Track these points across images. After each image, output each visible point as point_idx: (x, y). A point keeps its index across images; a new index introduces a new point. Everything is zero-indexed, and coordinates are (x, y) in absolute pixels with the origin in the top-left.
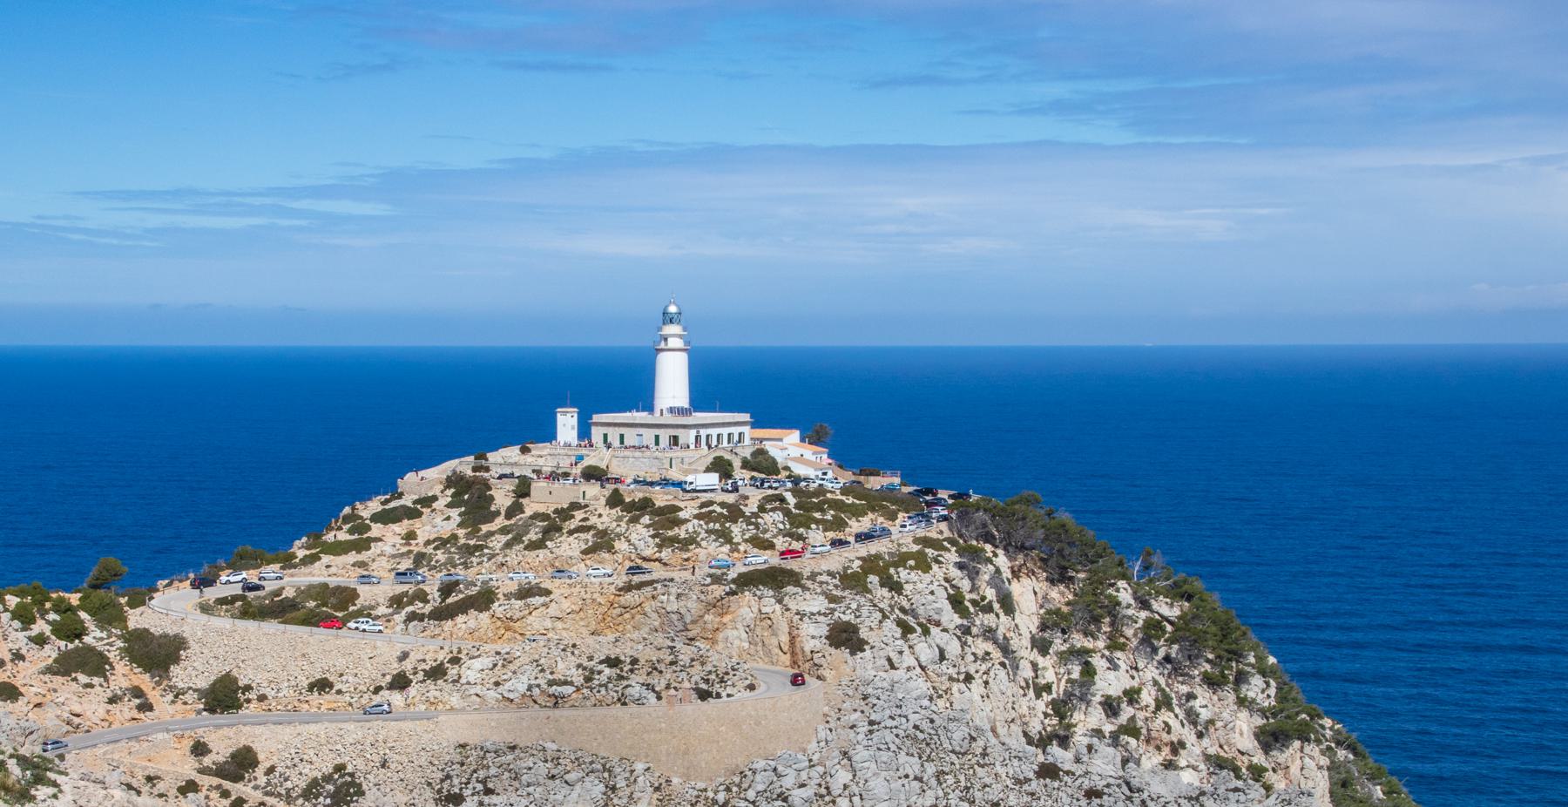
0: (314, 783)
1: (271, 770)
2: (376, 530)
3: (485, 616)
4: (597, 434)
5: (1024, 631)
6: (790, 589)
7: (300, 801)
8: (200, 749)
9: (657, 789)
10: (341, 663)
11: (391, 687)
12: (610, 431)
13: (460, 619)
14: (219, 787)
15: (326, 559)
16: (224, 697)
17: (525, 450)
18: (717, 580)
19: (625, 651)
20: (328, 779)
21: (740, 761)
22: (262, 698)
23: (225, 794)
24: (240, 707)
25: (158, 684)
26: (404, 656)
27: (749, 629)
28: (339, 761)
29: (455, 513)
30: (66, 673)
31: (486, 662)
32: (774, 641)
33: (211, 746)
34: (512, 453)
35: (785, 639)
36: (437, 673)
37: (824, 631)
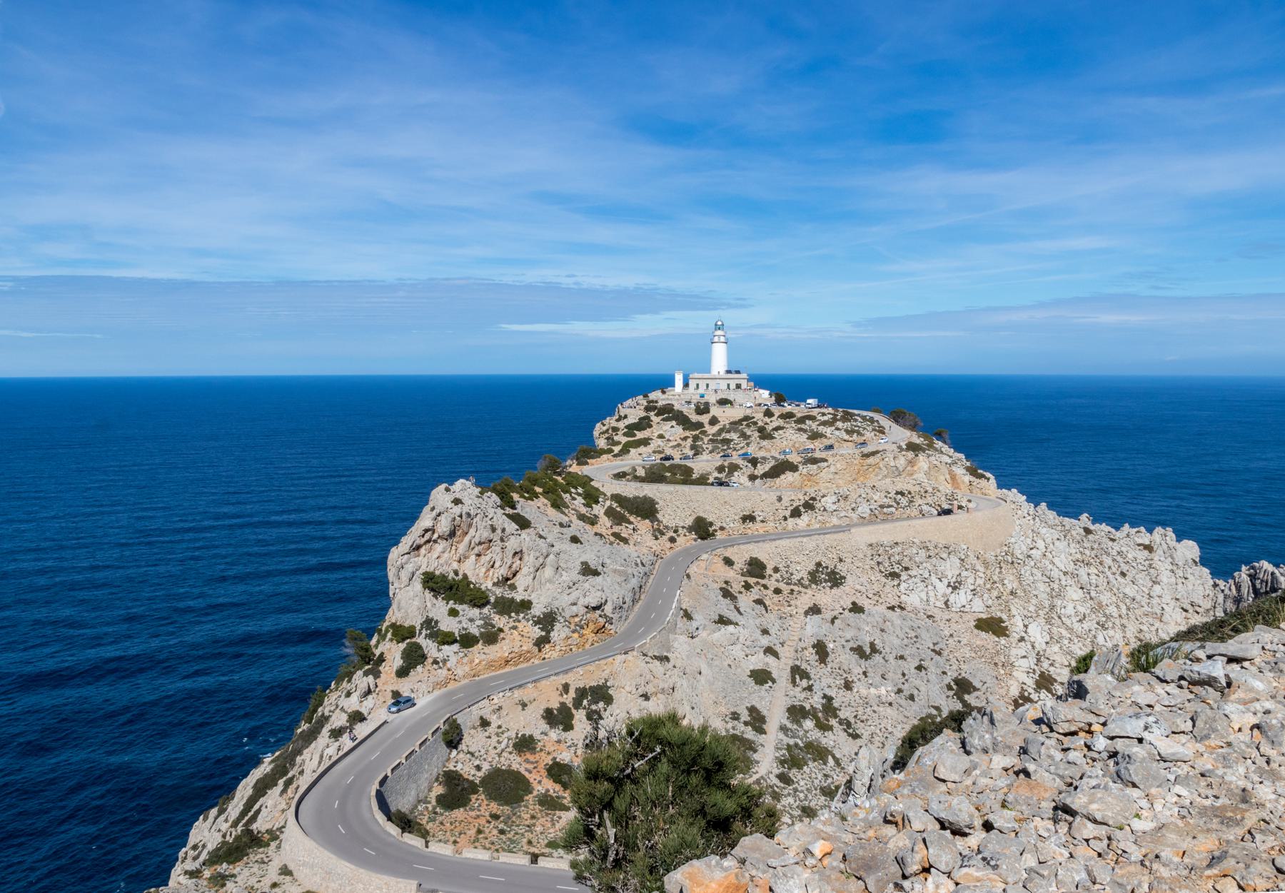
1: (776, 570)
3: (796, 474)
8: (728, 562)
10: (748, 505)
12: (700, 382)
17: (664, 392)
23: (765, 587)
32: (942, 478)
35: (948, 477)
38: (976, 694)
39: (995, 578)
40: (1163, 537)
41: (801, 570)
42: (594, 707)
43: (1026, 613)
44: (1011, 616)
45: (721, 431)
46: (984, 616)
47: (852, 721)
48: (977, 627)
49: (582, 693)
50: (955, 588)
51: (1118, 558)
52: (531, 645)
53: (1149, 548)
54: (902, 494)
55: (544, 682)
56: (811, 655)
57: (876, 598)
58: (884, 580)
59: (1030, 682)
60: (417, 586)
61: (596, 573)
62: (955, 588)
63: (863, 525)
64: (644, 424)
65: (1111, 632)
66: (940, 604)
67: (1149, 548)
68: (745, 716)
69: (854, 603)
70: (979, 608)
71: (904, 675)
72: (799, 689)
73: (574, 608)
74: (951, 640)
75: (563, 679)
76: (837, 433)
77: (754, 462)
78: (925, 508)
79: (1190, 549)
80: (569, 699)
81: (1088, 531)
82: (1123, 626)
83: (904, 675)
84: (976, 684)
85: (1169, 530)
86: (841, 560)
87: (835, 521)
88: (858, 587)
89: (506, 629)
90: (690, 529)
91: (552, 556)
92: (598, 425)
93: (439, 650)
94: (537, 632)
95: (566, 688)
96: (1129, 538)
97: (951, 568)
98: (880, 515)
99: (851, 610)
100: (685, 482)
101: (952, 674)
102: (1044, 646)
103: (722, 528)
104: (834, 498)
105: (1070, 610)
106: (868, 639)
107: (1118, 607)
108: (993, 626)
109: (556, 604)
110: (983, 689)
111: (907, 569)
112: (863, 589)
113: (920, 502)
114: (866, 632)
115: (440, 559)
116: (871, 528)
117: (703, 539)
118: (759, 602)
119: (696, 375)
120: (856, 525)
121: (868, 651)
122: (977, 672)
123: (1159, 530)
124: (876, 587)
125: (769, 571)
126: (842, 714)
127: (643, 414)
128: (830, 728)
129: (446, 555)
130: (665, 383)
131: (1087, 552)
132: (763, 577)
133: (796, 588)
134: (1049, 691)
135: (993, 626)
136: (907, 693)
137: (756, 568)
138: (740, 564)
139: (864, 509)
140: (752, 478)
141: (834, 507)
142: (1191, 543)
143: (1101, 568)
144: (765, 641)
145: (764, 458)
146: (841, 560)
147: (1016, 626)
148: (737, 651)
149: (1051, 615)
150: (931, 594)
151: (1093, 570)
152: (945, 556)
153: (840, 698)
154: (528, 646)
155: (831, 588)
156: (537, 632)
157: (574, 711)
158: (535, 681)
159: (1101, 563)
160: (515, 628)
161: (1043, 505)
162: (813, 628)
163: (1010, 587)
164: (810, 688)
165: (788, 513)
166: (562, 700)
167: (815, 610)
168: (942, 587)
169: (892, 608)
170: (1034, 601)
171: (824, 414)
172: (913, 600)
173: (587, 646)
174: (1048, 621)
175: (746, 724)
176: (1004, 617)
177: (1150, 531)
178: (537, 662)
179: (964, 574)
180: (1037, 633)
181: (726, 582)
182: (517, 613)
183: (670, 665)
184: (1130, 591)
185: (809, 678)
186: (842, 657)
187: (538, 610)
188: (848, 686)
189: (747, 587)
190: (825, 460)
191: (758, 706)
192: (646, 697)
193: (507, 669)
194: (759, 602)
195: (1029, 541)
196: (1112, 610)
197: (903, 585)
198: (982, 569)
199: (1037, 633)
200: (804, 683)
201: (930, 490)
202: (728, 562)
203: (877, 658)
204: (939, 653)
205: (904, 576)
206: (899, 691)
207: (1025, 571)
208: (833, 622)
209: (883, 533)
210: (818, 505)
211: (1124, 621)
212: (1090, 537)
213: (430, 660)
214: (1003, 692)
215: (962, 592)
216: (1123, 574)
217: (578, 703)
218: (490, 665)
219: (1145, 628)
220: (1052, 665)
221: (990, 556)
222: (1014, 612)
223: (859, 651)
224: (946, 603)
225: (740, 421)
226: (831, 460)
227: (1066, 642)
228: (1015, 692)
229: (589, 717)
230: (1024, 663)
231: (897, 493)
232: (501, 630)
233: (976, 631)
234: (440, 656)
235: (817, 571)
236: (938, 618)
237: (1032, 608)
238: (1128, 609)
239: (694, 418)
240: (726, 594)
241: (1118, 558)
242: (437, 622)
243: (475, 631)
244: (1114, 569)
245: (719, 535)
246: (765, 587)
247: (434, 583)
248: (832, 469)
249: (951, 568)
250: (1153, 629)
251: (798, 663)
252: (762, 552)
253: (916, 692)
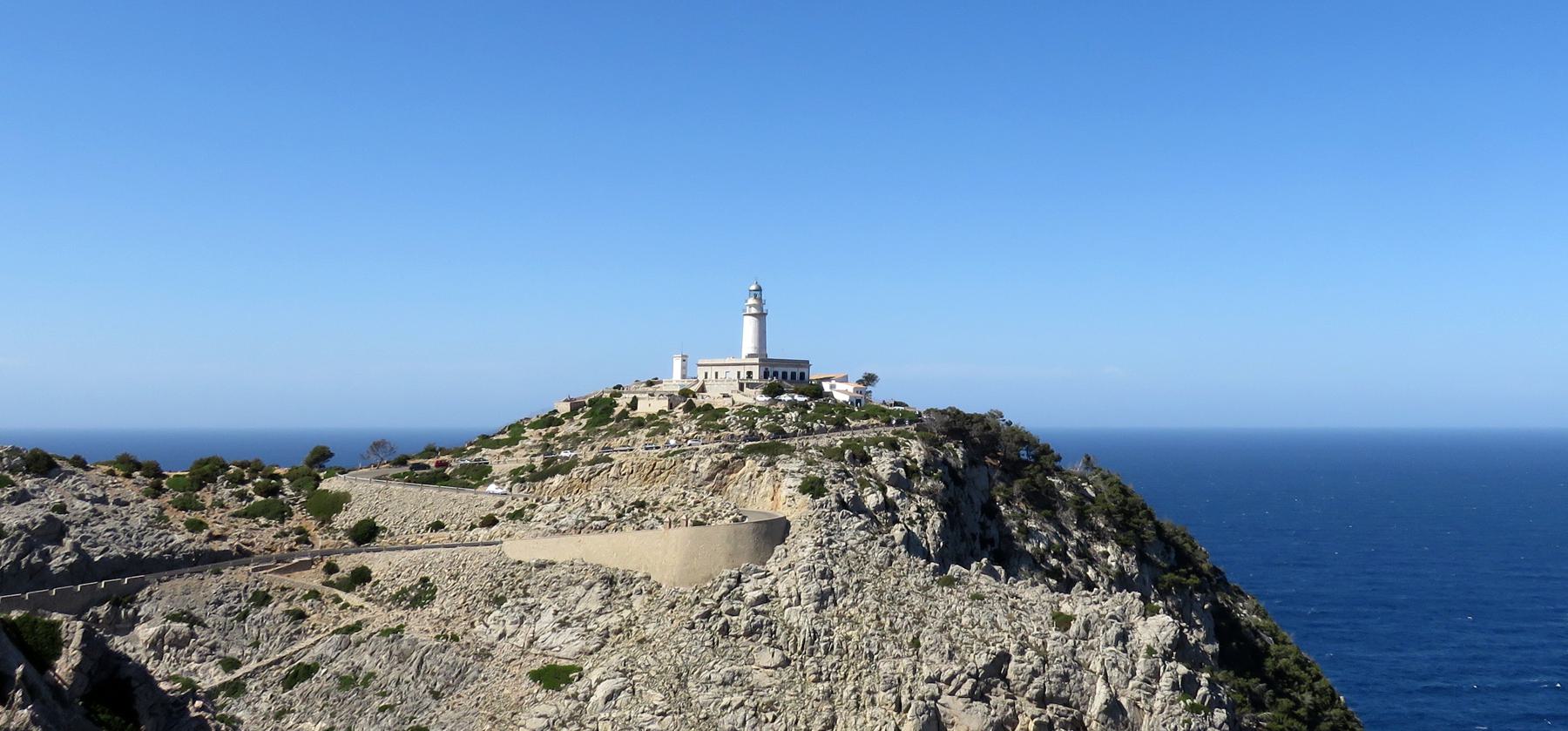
0: (404, 591)
2: (529, 432)
5: (976, 500)
6: (783, 456)
9: (650, 592)
11: (482, 525)
13: (549, 480)
15: (484, 451)
16: (366, 534)
18: (728, 449)
19: (648, 497)
20: (411, 588)
22: (391, 535)
25: (321, 525)
26: (501, 504)
28: (423, 574)
29: (584, 422)
31: (552, 506)
36: (517, 515)
37: (799, 483)
155: (406, 608)
197: (497, 613)
205: (509, 603)
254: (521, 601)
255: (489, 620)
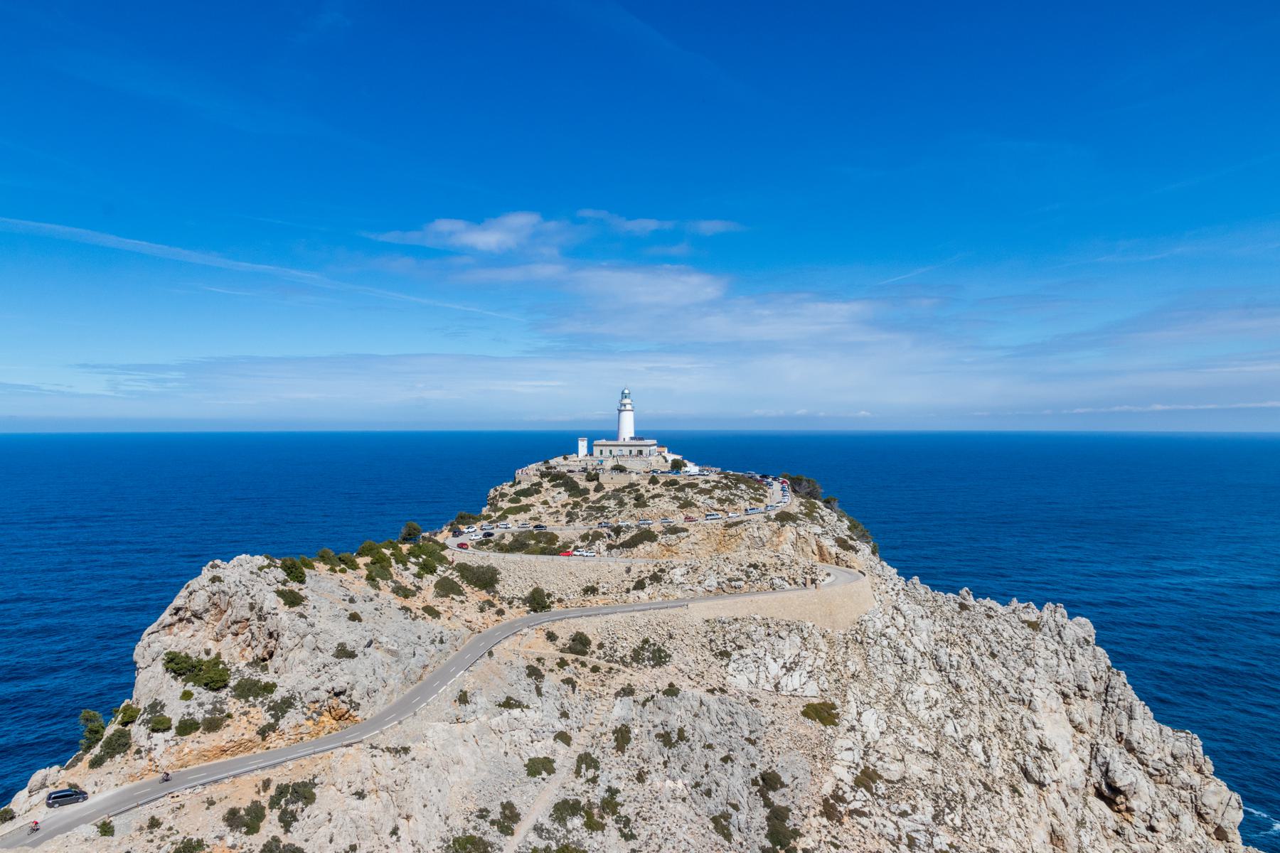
1: (601, 646)
3: (655, 544)
4: (596, 451)
7: (635, 664)
8: (551, 637)
10: (594, 577)
11: (635, 588)
14: (577, 660)
15: (511, 517)
16: (538, 602)
17: (565, 459)
21: (855, 617)
23: (583, 664)
24: (549, 607)
27: (794, 545)
30: (447, 596)
33: (557, 633)
34: (560, 459)
35: (815, 548)
38: (784, 790)
39: (839, 659)
40: (1053, 614)
41: (624, 649)
42: (291, 807)
43: (864, 698)
44: (846, 702)
45: (603, 497)
46: (815, 701)
47: (633, 819)
48: (804, 714)
49: (282, 790)
50: (788, 670)
51: (992, 638)
52: (254, 733)
53: (1034, 626)
54: (755, 566)
55: (244, 777)
56: (609, 741)
57: (698, 679)
58: (712, 659)
59: (849, 779)
60: (159, 667)
61: (352, 655)
62: (789, 669)
63: (708, 598)
64: (535, 489)
65: (964, 721)
66: (769, 687)
67: (1034, 626)
68: (496, 814)
69: (671, 685)
70: (812, 692)
71: (707, 766)
72: (583, 780)
73: (315, 693)
74: (771, 728)
75: (265, 775)
76: (709, 501)
77: (618, 531)
78: (777, 581)
79: (1082, 627)
80: (264, 799)
81: (963, 607)
82: (983, 713)
83: (707, 766)
84: (786, 779)
85: (1062, 610)
86: (671, 637)
87: (679, 594)
88: (682, 666)
89: (236, 716)
90: (525, 601)
91: (309, 637)
92: (492, 490)
93: (149, 738)
94: (264, 718)
95: (266, 784)
96: (1007, 619)
97: (790, 647)
98: (729, 587)
99: (665, 693)
100: (543, 552)
101: (761, 768)
102: (877, 736)
103: (560, 601)
104: (684, 570)
105: (919, 694)
106: (678, 725)
107: (980, 692)
108: (823, 713)
109: (301, 688)
110: (792, 787)
111: (740, 647)
112: (687, 669)
113: (773, 575)
114: (677, 716)
115: (193, 641)
116: (709, 603)
117: (535, 611)
118: (568, 681)
119: (603, 442)
120: (701, 599)
121: (675, 737)
122: (789, 765)
123: (1050, 605)
124: (701, 668)
125: (594, 647)
126: (622, 811)
127: (536, 480)
128: (602, 827)
129: (200, 634)
130: (566, 445)
131: (954, 630)
132: (585, 653)
133: (616, 666)
134: (869, 789)
135: (823, 713)
136: (703, 788)
137: (580, 644)
138: (564, 638)
139: (712, 581)
140: (610, 547)
141: (682, 580)
142: (1083, 620)
143: (966, 648)
144: (560, 726)
145: (628, 527)
146: (671, 637)
147: (848, 714)
148: (522, 736)
149: (895, 701)
150: (762, 675)
151: (958, 651)
152: (783, 634)
153: (627, 790)
154: (251, 734)
155: (653, 667)
156: (264, 718)
157: (267, 811)
158: (234, 776)
159: (969, 643)
160: (246, 714)
161: (916, 579)
162: (620, 710)
163: (852, 669)
164: (594, 780)
165: (632, 585)
166: (256, 798)
167: (628, 691)
168: (775, 669)
169: (712, 691)
170: (877, 685)
171: (707, 482)
172: (739, 682)
173: (322, 735)
174: (889, 709)
175: (493, 823)
176: (838, 703)
177: (1040, 606)
178: (259, 752)
179: (803, 653)
180: (872, 722)
181: (539, 660)
182: (256, 697)
183: (408, 758)
184: (997, 674)
185: (597, 768)
186: (644, 743)
187: (277, 696)
188: (641, 778)
189: (562, 664)
190: (686, 530)
191: (515, 801)
192: (360, 795)
193: (224, 759)
194: (568, 681)
195: (887, 618)
196: (974, 696)
197: (732, 665)
198: (825, 649)
199: (872, 722)
200: (590, 773)
201: (787, 561)
202: (551, 637)
203: (683, 747)
204: (753, 743)
205: (735, 655)
206: (697, 785)
207: (875, 652)
208: (644, 705)
209: (724, 608)
210: (666, 577)
211: (984, 708)
212: (964, 614)
213: (134, 748)
214: (814, 789)
215: (796, 674)
216: (993, 655)
217: (274, 803)
218: (202, 755)
219: (1008, 716)
220: (880, 759)
221: (838, 634)
222: (850, 697)
223: (665, 739)
224: (776, 686)
225: (623, 490)
226: (691, 530)
227: (904, 732)
228: (828, 789)
229: (281, 820)
230: (848, 756)
231: (750, 566)
232: (230, 716)
233: (802, 718)
234: (145, 743)
235: (642, 648)
236: (763, 702)
237: (872, 693)
238: (992, 693)
239: (583, 484)
240: (534, 673)
241: (992, 638)
242: (163, 707)
243: (199, 715)
244: (983, 649)
245: (556, 607)
246: (583, 664)
247: (178, 666)
248: (692, 539)
249: (790, 647)
250: (1017, 717)
251: (590, 750)
252: (591, 628)
253: (714, 787)
254: (742, 652)
255: (730, 669)
